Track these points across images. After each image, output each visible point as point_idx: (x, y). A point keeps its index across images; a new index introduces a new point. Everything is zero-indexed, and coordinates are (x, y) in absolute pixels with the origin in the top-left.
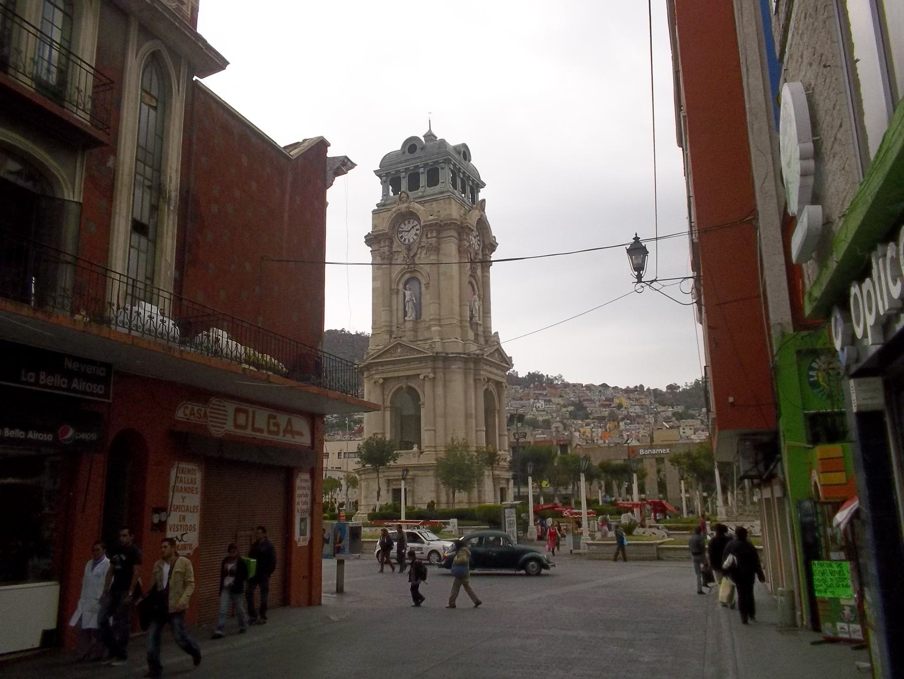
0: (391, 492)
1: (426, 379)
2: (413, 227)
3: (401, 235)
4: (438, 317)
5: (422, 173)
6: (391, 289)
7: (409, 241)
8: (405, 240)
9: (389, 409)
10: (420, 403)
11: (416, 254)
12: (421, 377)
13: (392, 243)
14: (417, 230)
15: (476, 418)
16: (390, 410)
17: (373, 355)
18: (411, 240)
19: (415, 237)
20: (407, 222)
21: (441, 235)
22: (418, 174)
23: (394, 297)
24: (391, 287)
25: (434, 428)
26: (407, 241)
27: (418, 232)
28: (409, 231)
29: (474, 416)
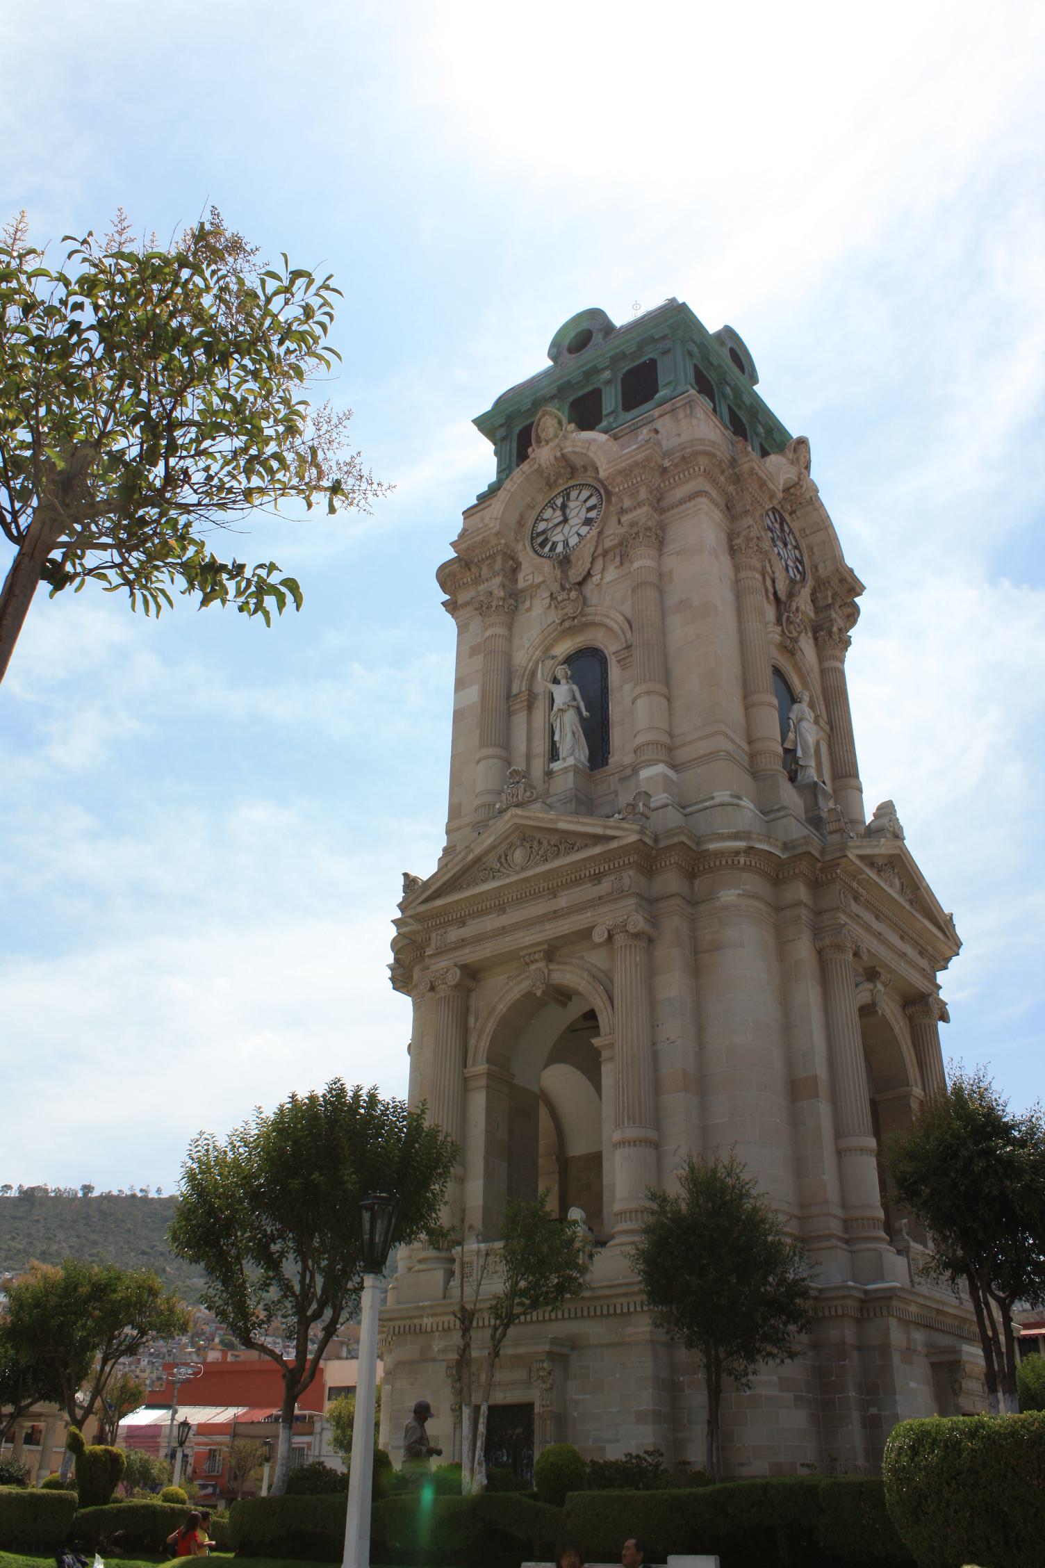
1: (620, 939)
3: (540, 540)
4: (665, 739)
5: (608, 382)
7: (566, 544)
8: (553, 548)
9: (483, 1082)
10: (596, 1042)
11: (589, 575)
12: (599, 936)
13: (515, 570)
15: (834, 1100)
16: (488, 1087)
18: (573, 541)
19: (584, 530)
21: (665, 503)
22: (597, 394)
23: (520, 720)
24: (509, 689)
25: (651, 1134)
26: (560, 548)
27: (592, 514)
28: (565, 520)
29: (823, 1089)
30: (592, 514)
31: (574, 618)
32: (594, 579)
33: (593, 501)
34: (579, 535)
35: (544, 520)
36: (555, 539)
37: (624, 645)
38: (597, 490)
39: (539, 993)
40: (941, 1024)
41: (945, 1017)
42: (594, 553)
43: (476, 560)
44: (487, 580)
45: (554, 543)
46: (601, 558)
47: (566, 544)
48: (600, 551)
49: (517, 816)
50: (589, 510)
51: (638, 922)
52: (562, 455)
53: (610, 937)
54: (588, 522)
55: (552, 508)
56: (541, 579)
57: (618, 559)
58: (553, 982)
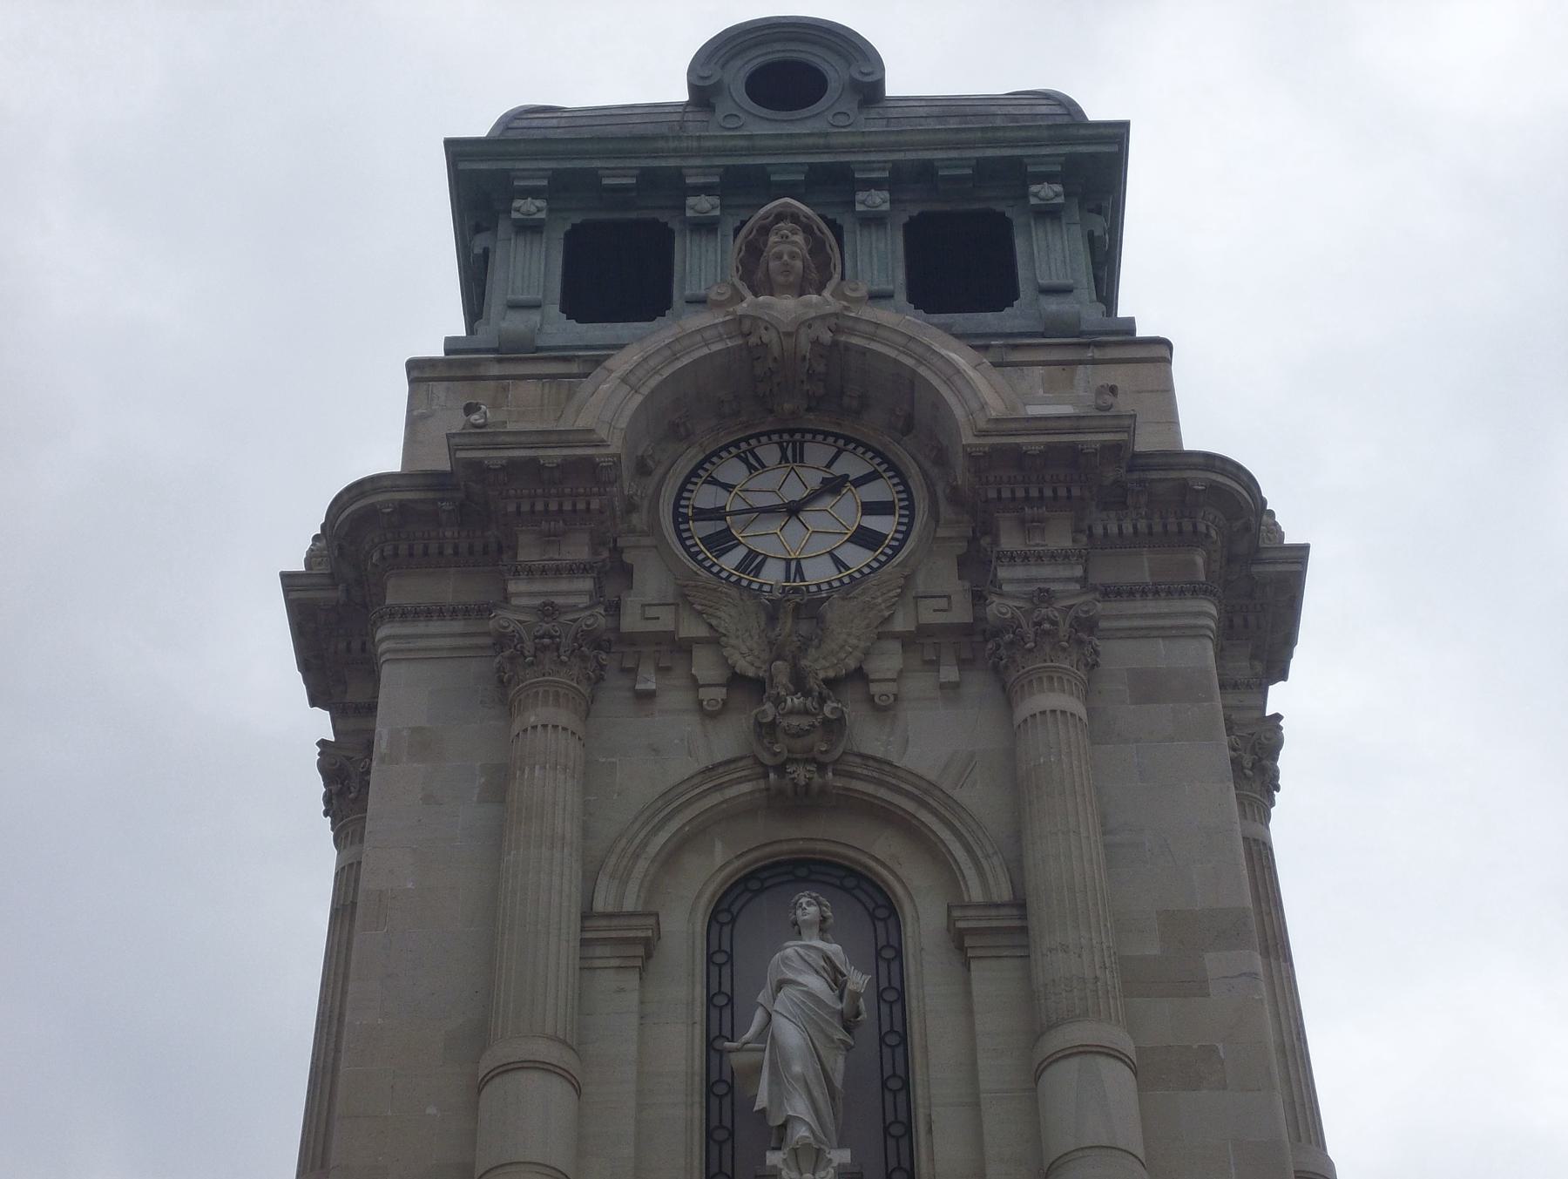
2: (833, 486)
6: (587, 915)
14: (869, 508)
19: (858, 558)
20: (769, 454)
24: (589, 898)
26: (772, 574)
27: (884, 525)
30: (884, 525)
31: (822, 768)
33: (879, 491)
34: (839, 564)
35: (713, 481)
36: (760, 546)
43: (511, 508)
44: (530, 571)
45: (752, 554)
46: (895, 646)
47: (794, 568)
50: (869, 508)
52: (835, 344)
54: (865, 538)
55: (746, 461)
56: (702, 631)
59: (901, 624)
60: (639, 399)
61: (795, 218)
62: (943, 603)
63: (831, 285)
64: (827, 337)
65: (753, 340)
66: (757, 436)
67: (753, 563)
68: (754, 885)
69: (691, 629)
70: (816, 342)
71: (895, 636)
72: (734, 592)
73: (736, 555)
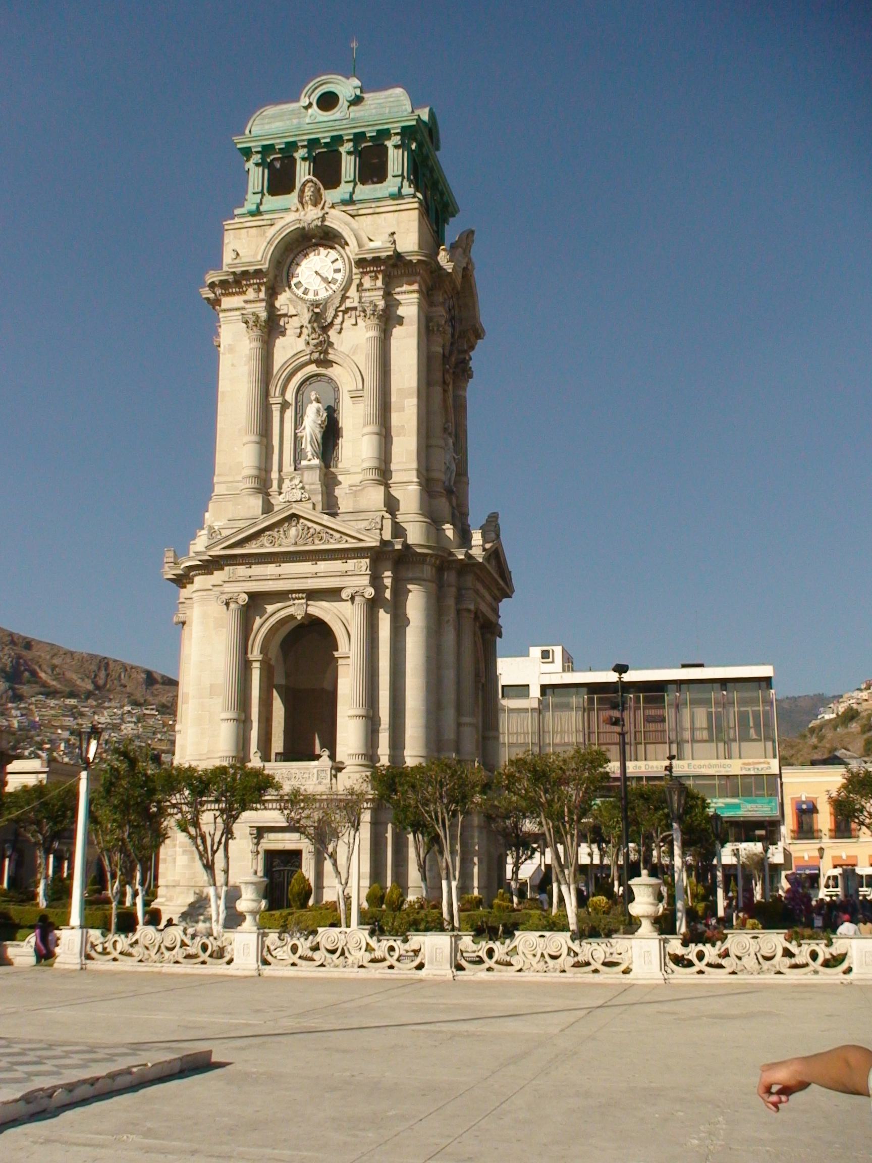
0: (261, 856)
11: (331, 324)
17: (227, 538)
32: (335, 327)
33: (339, 265)
37: (355, 388)
38: (342, 256)
39: (299, 618)
40: (498, 639)
41: (500, 636)
42: (338, 308)
46: (340, 314)
48: (342, 308)
49: (295, 508)
50: (337, 271)
51: (370, 592)
53: (352, 599)
56: (295, 313)
57: (354, 316)
58: (308, 612)
59: (341, 309)
60: (272, 248)
61: (312, 181)
62: (351, 300)
63: (320, 206)
64: (319, 224)
65: (301, 226)
66: (308, 248)
67: (306, 292)
68: (301, 392)
69: (292, 311)
70: (317, 226)
71: (340, 311)
72: (300, 302)
73: (302, 289)
